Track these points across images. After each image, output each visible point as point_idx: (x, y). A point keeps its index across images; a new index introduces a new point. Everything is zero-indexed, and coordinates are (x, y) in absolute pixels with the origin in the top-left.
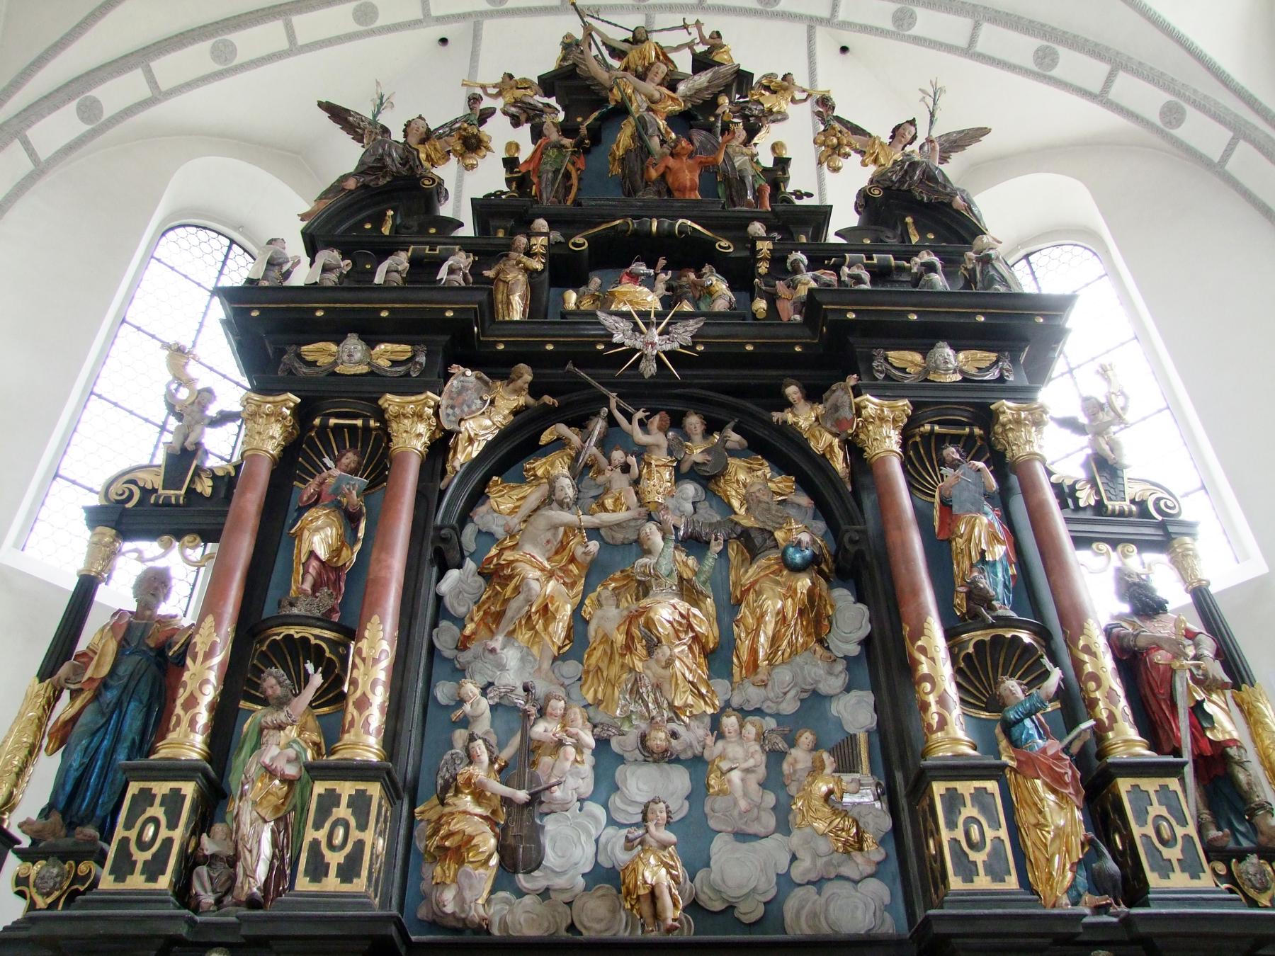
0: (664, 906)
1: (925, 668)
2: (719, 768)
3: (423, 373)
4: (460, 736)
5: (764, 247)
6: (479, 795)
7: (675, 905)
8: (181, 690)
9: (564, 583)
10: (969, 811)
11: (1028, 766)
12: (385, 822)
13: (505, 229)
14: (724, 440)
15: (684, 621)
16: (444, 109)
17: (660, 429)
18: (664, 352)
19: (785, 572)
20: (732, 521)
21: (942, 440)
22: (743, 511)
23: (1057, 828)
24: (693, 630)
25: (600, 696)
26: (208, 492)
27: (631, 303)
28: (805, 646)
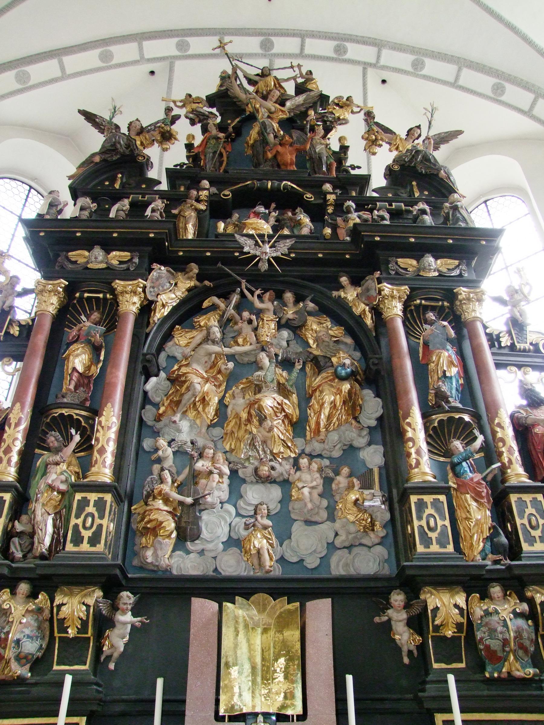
0: (264, 559)
1: (410, 434)
2: (297, 487)
3: (138, 267)
4: (156, 468)
5: (331, 198)
6: (166, 500)
7: (271, 559)
8: (3, 444)
9: (215, 385)
10: (430, 511)
11: (463, 487)
12: (114, 514)
13: (184, 185)
14: (305, 307)
15: (280, 407)
16: (151, 116)
17: (270, 300)
18: (272, 257)
19: (336, 380)
20: (308, 351)
21: (426, 308)
22: (315, 346)
23: (477, 520)
24: (284, 411)
25: (233, 447)
26: (17, 334)
27: (255, 229)
28: (346, 421)
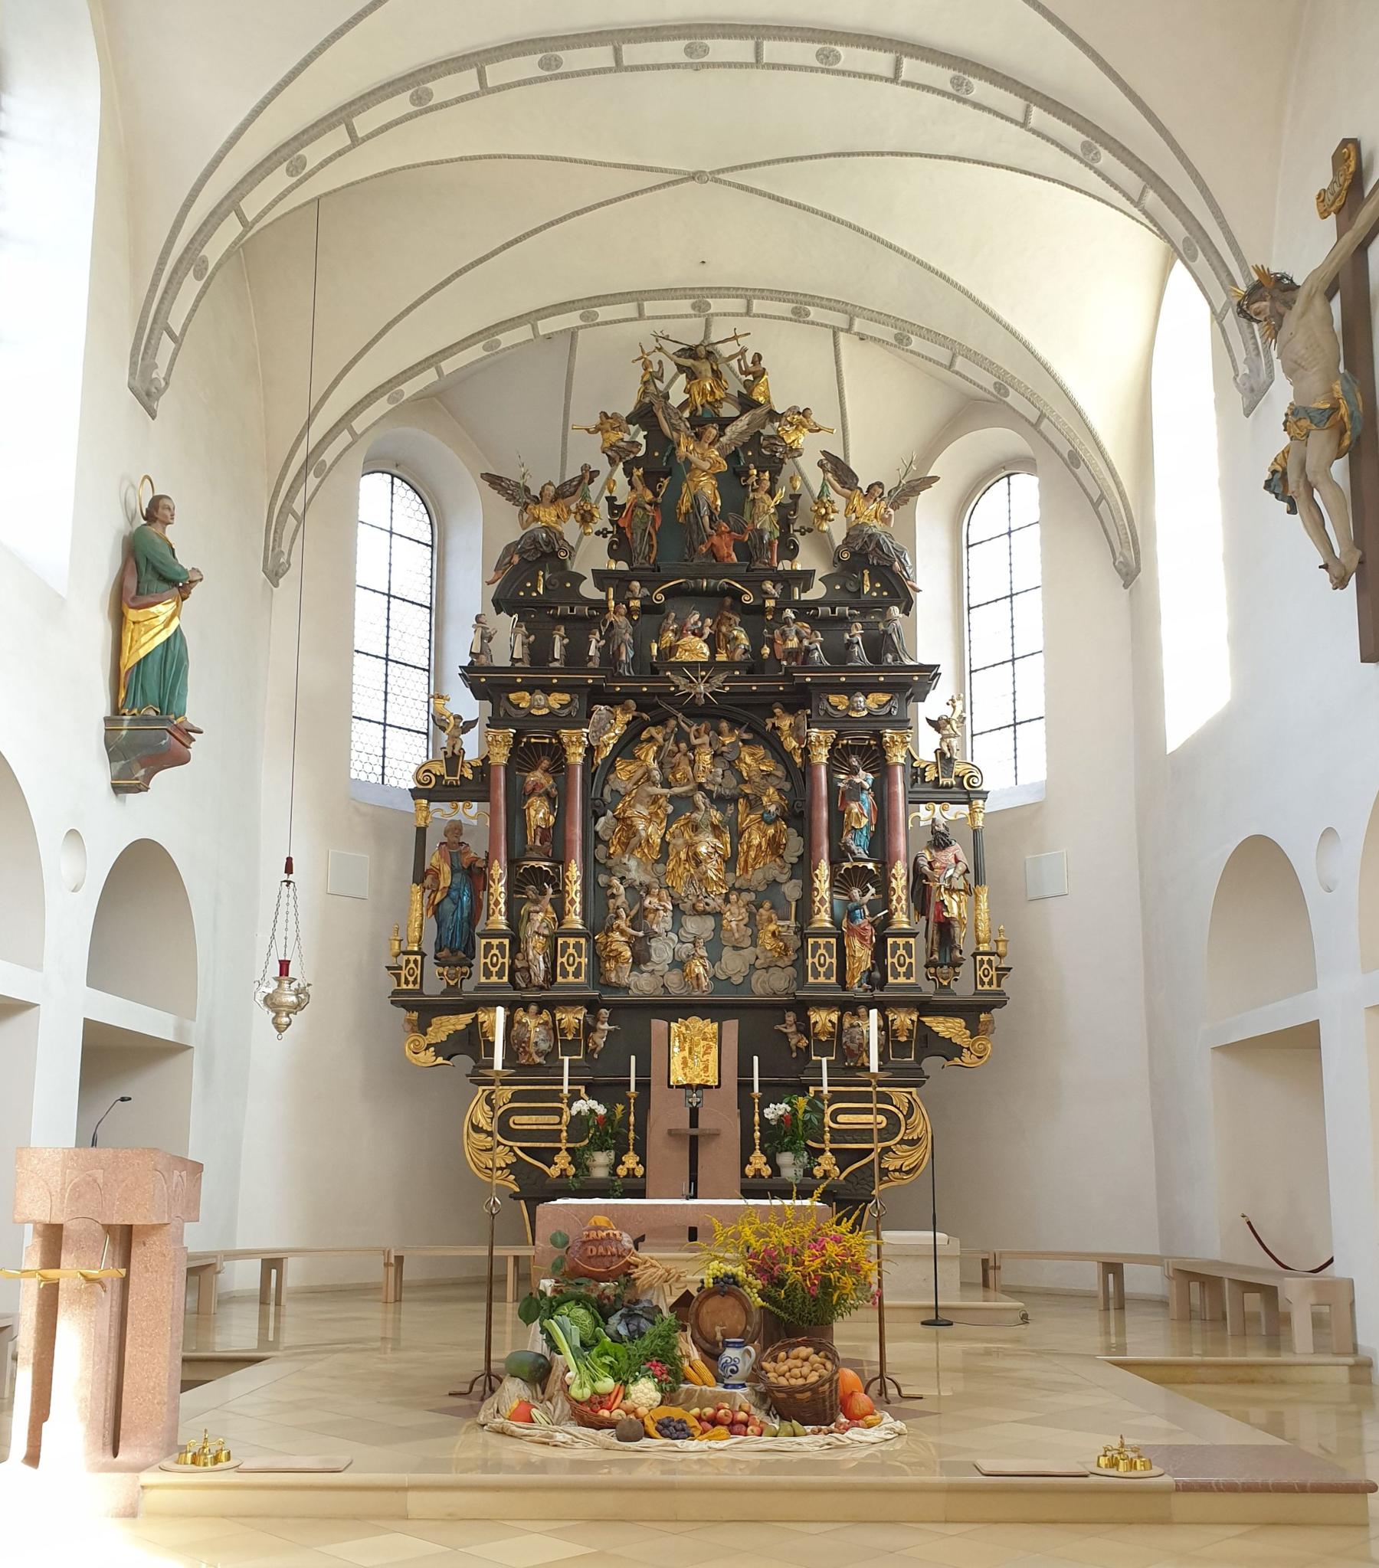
1: (817, 884)
6: (623, 933)
10: (822, 951)
26: (470, 777)
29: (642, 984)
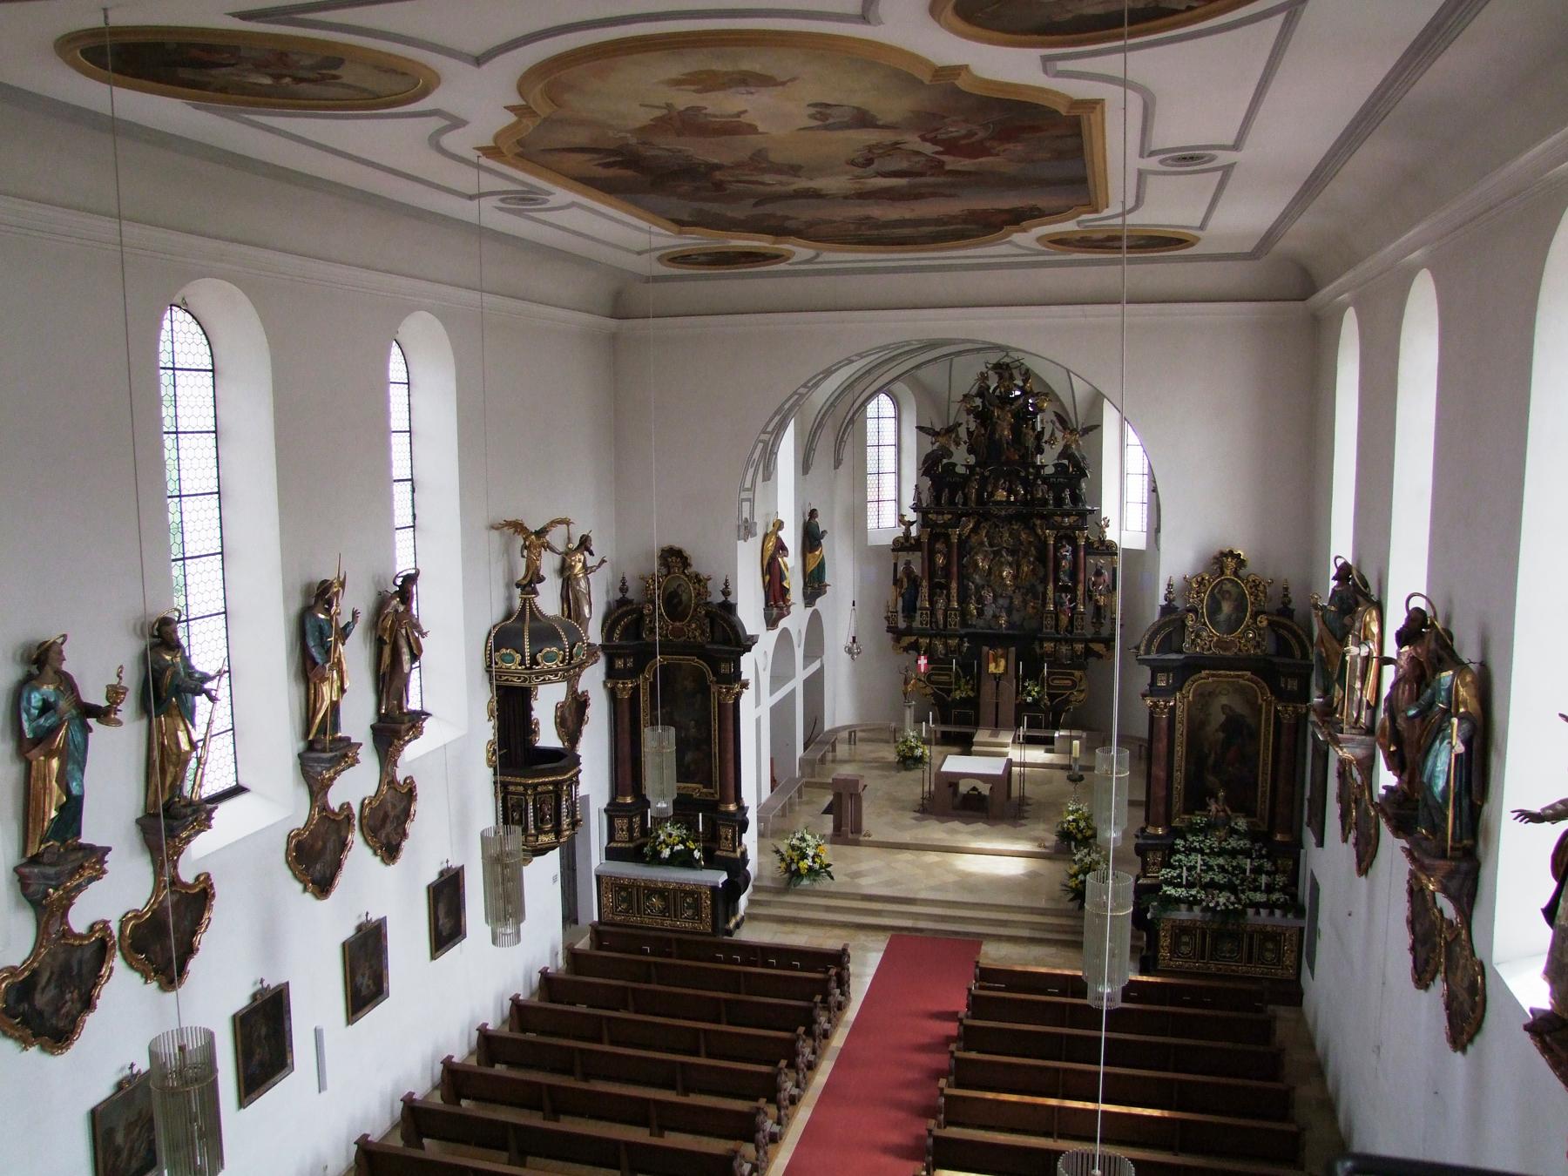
29: (979, 625)
